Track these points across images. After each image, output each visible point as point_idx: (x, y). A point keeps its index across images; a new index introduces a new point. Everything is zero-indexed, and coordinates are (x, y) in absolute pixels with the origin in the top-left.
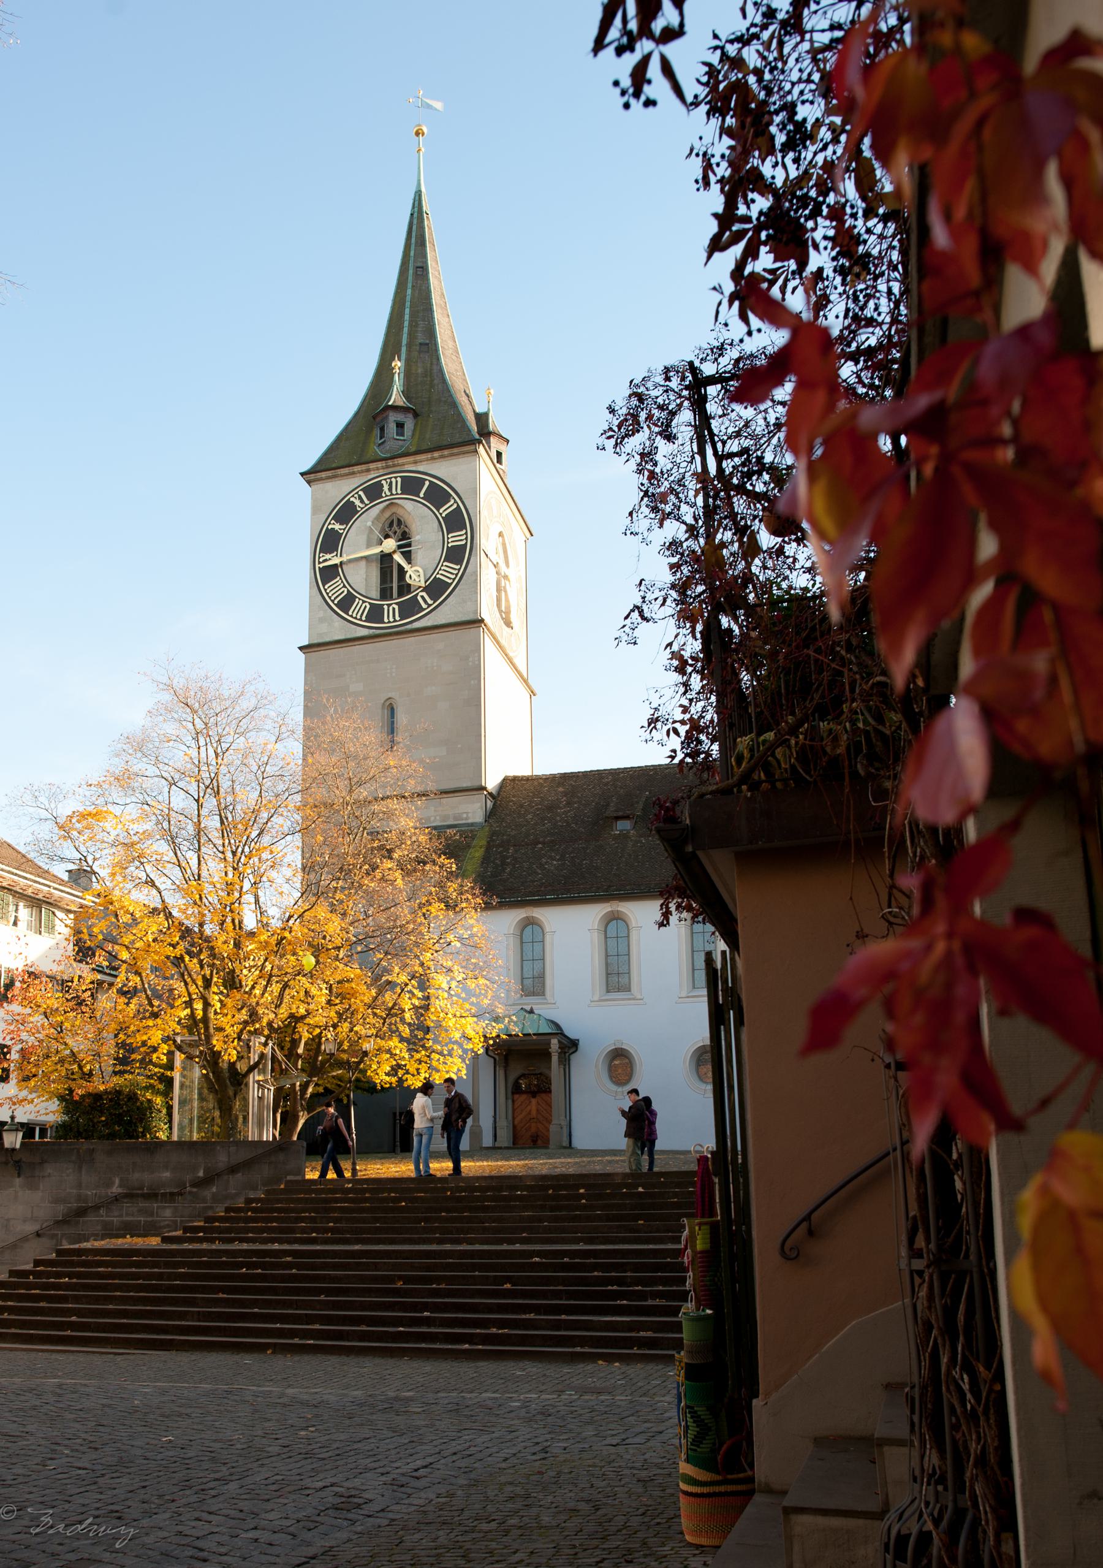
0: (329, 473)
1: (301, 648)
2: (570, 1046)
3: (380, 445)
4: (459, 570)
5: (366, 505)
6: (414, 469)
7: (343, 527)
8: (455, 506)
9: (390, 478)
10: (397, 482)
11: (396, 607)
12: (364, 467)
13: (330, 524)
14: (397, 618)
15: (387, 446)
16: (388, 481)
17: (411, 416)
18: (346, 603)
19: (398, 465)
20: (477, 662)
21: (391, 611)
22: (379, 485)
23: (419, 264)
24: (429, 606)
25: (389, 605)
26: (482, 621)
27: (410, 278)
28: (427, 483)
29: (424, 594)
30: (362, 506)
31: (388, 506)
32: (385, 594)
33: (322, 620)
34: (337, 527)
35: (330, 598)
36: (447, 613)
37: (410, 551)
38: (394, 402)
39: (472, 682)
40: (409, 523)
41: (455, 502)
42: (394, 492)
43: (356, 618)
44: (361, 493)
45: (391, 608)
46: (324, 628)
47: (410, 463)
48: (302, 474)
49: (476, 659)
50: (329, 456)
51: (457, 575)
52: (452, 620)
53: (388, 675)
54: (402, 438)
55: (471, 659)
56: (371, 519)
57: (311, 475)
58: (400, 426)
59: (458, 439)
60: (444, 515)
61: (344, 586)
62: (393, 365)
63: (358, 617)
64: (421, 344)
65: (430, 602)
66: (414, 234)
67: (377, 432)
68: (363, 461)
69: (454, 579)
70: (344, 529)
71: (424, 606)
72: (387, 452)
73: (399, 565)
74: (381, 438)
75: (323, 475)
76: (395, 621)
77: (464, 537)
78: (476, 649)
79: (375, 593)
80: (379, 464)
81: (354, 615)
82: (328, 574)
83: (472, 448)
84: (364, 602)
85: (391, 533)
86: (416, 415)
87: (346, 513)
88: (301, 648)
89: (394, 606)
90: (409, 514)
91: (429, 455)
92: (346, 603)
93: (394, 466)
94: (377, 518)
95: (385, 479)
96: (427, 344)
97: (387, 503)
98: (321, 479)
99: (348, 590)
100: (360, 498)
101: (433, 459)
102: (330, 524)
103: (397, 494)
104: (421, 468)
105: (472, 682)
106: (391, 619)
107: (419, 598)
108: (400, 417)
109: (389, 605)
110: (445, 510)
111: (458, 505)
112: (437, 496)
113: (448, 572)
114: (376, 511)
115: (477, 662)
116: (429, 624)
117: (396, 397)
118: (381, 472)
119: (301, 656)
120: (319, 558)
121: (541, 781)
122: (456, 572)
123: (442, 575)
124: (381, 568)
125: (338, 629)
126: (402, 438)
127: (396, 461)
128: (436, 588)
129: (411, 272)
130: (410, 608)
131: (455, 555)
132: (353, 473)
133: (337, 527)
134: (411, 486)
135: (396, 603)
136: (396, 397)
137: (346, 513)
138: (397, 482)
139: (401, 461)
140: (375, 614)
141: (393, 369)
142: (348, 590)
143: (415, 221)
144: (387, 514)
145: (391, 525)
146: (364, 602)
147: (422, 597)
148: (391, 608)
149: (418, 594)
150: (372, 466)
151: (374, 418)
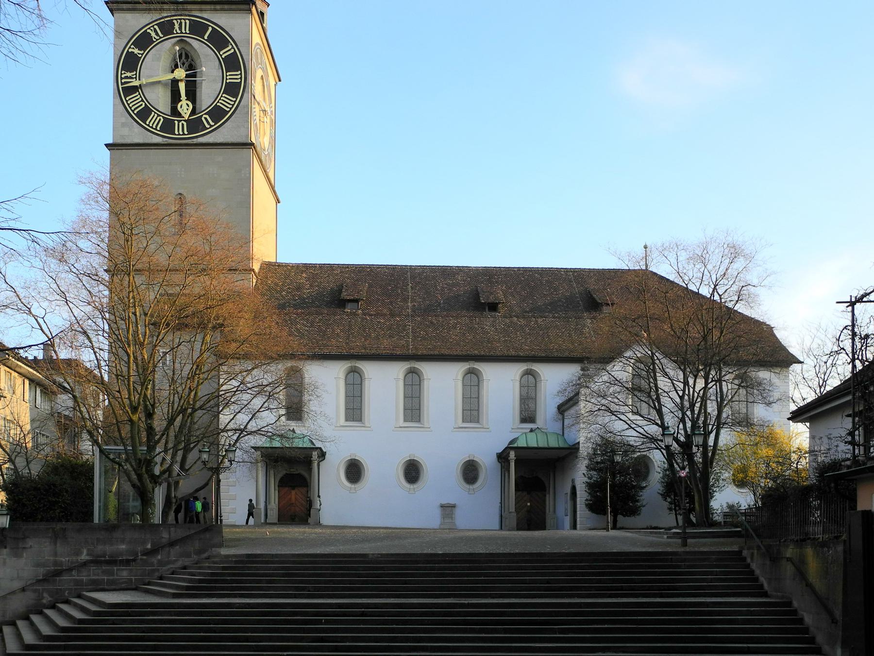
1: (107, 145)
4: (235, 102)
5: (161, 38)
8: (232, 51)
10: (186, 23)
12: (159, 6)
14: (186, 132)
16: (179, 21)
18: (144, 114)
20: (248, 175)
24: (211, 126)
25: (179, 121)
26: (252, 144)
28: (210, 29)
29: (207, 116)
30: (158, 38)
33: (124, 125)
34: (136, 51)
35: (130, 108)
36: (224, 134)
37: (196, 80)
39: (244, 190)
40: (195, 58)
41: (233, 48)
44: (156, 27)
45: (180, 124)
46: (125, 131)
49: (247, 172)
51: (233, 105)
53: (179, 176)
55: (243, 172)
61: (142, 100)
63: (154, 127)
65: (212, 124)
69: (231, 109)
70: (142, 54)
71: (208, 126)
76: (184, 134)
77: (239, 76)
78: (249, 166)
79: (168, 111)
87: (144, 41)
88: (107, 145)
97: (178, 39)
98: (123, 10)
100: (155, 30)
101: (216, 10)
102: (130, 48)
103: (186, 33)
104: (205, 15)
105: (244, 190)
106: (181, 133)
107: (203, 119)
109: (179, 121)
110: (225, 52)
112: (219, 40)
113: (226, 102)
114: (168, 44)
115: (248, 175)
118: (173, 13)
119: (107, 152)
120: (121, 74)
125: (137, 134)
127: (186, 6)
128: (217, 114)
131: (232, 89)
132: (150, 10)
133: (136, 51)
134: (198, 29)
137: (144, 41)
138: (186, 23)
139: (189, 7)
140: (168, 127)
146: (159, 115)
147: (206, 118)
149: (203, 115)
150: (165, 6)
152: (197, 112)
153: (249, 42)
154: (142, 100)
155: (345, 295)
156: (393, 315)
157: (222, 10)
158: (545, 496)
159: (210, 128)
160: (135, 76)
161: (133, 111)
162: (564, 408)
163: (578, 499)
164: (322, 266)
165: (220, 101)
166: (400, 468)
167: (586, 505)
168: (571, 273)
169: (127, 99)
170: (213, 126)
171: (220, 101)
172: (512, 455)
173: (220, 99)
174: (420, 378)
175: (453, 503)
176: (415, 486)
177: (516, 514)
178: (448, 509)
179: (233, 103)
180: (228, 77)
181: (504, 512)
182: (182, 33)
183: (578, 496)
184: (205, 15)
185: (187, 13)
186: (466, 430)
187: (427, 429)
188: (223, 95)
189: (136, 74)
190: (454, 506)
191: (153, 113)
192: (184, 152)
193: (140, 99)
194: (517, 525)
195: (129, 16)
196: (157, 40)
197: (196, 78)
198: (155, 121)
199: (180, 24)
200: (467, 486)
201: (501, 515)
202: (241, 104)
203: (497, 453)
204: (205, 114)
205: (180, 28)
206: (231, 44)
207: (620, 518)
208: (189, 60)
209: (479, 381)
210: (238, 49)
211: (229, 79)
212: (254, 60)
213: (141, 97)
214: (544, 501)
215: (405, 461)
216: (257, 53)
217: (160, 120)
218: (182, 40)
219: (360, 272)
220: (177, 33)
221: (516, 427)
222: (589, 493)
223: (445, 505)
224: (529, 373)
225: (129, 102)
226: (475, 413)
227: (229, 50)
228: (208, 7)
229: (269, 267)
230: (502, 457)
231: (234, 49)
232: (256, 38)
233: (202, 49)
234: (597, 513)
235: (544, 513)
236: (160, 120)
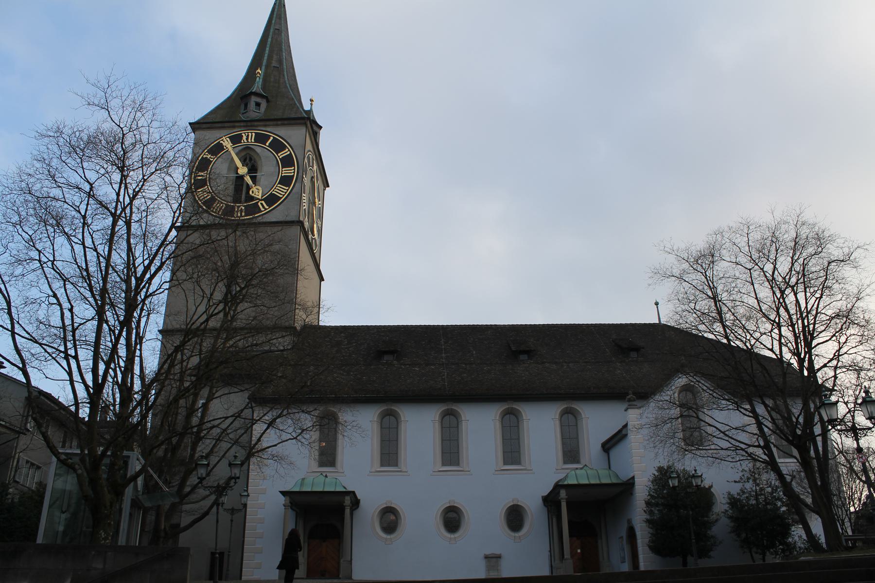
2: (356, 503)
3: (243, 114)
4: (288, 190)
6: (264, 129)
8: (289, 152)
10: (252, 135)
13: (205, 154)
15: (247, 115)
16: (247, 134)
17: (265, 100)
22: (240, 136)
23: (278, 28)
24: (266, 209)
26: (301, 224)
27: (271, 34)
28: (272, 138)
29: (263, 202)
31: (244, 148)
32: (237, 200)
34: (209, 156)
41: (289, 150)
50: (209, 116)
51: (286, 193)
57: (195, 126)
58: (258, 105)
59: (293, 116)
64: (274, 67)
66: (275, 13)
67: (243, 107)
68: (233, 119)
69: (284, 195)
71: (263, 209)
72: (248, 117)
73: (248, 184)
74: (245, 110)
75: (204, 126)
80: (242, 124)
83: (302, 121)
86: (268, 101)
90: (258, 154)
91: (275, 123)
92: (209, 203)
93: (251, 126)
95: (245, 133)
96: (278, 67)
97: (244, 146)
101: (277, 125)
102: (205, 154)
103: (251, 142)
104: (269, 129)
107: (259, 204)
108: (259, 100)
110: (282, 154)
111: (291, 152)
112: (277, 146)
113: (280, 191)
117: (257, 86)
121: (329, 329)
123: (276, 192)
128: (271, 199)
129: (272, 30)
133: (209, 156)
134: (261, 139)
136: (257, 86)
138: (252, 135)
139: (256, 124)
143: (277, 7)
147: (262, 204)
150: (237, 124)
151: (242, 98)
159: (265, 211)
162: (607, 446)
165: (275, 190)
171: (275, 190)
173: (275, 188)
175: (498, 552)
176: (457, 535)
178: (493, 559)
180: (283, 172)
182: (248, 142)
184: (269, 129)
185: (254, 128)
186: (508, 472)
187: (466, 473)
188: (278, 186)
190: (499, 557)
197: (256, 173)
199: (248, 136)
200: (513, 534)
201: (551, 565)
202: (293, 191)
203: (542, 497)
206: (288, 148)
208: (252, 162)
209: (518, 422)
211: (284, 173)
212: (306, 160)
215: (444, 508)
216: (308, 158)
220: (244, 142)
223: (490, 556)
227: (286, 152)
228: (271, 123)
230: (551, 501)
231: (290, 151)
233: (263, 152)
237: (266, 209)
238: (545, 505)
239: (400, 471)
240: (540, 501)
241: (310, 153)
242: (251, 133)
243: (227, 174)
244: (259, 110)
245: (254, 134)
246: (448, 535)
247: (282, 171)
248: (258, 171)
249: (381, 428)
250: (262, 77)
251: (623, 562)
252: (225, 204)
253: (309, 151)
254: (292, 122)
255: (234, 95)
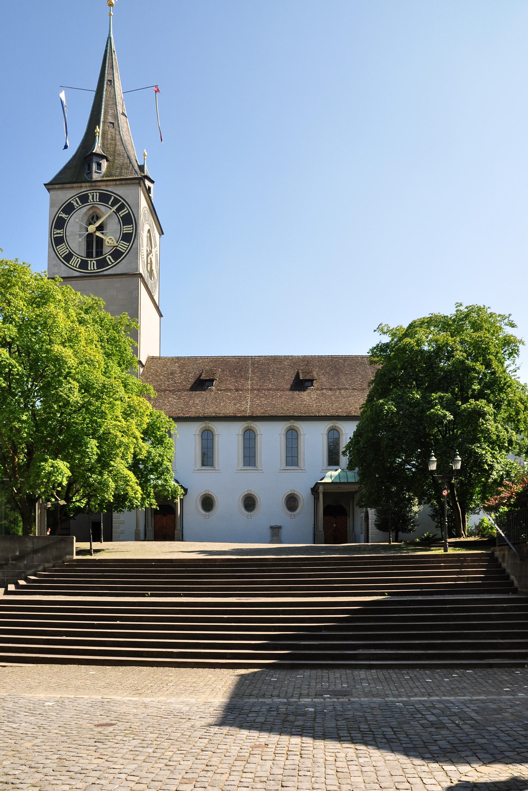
0: (60, 186)
3: (88, 174)
4: (129, 246)
7: (67, 216)
8: (127, 212)
9: (93, 193)
11: (95, 262)
12: (79, 185)
13: (60, 213)
16: (92, 194)
17: (105, 160)
18: (68, 257)
19: (97, 186)
21: (92, 264)
24: (113, 263)
25: (91, 261)
26: (141, 274)
28: (113, 198)
29: (110, 257)
30: (78, 206)
31: (91, 208)
32: (89, 254)
33: (55, 266)
34: (64, 216)
35: (59, 254)
38: (96, 151)
41: (128, 209)
42: (95, 200)
43: (73, 266)
44: (77, 199)
47: (103, 186)
48: (45, 185)
50: (60, 176)
51: (127, 248)
52: (124, 272)
54: (100, 171)
55: (134, 293)
56: (82, 214)
57: (50, 186)
60: (121, 216)
61: (67, 248)
62: (95, 131)
63: (75, 266)
65: (113, 261)
69: (126, 251)
70: (68, 218)
71: (110, 263)
74: (88, 170)
75: (57, 186)
76: (94, 270)
77: (132, 229)
78: (137, 288)
79: (84, 254)
80: (87, 184)
81: (72, 265)
82: (58, 241)
83: (137, 181)
84: (78, 258)
85: (92, 222)
87: (69, 209)
89: (94, 261)
90: (103, 213)
91: (114, 183)
92: (68, 257)
93: (95, 186)
94: (86, 213)
95: (90, 193)
97: (91, 206)
98: (55, 189)
99: (69, 251)
100: (76, 201)
101: (116, 185)
102: (60, 213)
103: (97, 201)
105: (134, 306)
106: (92, 269)
107: (107, 259)
109: (91, 261)
111: (129, 211)
113: (123, 246)
114: (85, 210)
116: (112, 273)
117: (97, 149)
120: (54, 231)
122: (127, 247)
124: (87, 241)
126: (100, 171)
128: (117, 254)
130: (102, 264)
131: (127, 238)
132: (73, 188)
133: (64, 216)
134: (104, 198)
135: (95, 260)
137: (69, 209)
139: (99, 184)
140: (84, 265)
141: (96, 133)
142: (69, 251)
144: (91, 212)
145: (93, 218)
146: (78, 258)
147: (109, 258)
148: (92, 262)
149: (106, 256)
150: (83, 185)
151: (85, 158)
152: (103, 254)
153: (138, 205)
154: (67, 248)
155: (203, 377)
156: (237, 390)
157: (121, 184)
158: (347, 519)
159: (112, 264)
160: (62, 232)
161: (61, 256)
163: (370, 521)
164: (189, 358)
166: (241, 499)
167: (375, 524)
168: (365, 359)
169: (57, 248)
170: (113, 263)
172: (321, 488)
174: (255, 433)
177: (323, 533)
179: (127, 247)
180: (124, 230)
181: (317, 531)
182: (94, 201)
183: (370, 518)
186: (289, 471)
189: (63, 231)
190: (280, 528)
191: (74, 256)
192: (94, 281)
193: (66, 248)
194: (325, 541)
195: (59, 193)
196: (77, 207)
197: (103, 230)
198: (75, 261)
200: (290, 513)
202: (133, 247)
203: (311, 488)
204: (109, 255)
205: (93, 199)
207: (400, 533)
209: (298, 435)
210: (131, 210)
211: (125, 230)
213: (66, 246)
214: (346, 523)
217: (78, 261)
218: (94, 206)
219: (215, 361)
221: (324, 469)
222: (378, 516)
224: (333, 430)
225: (58, 250)
226: (295, 459)
229: (151, 359)
232: (143, 203)
234: (383, 531)
235: (346, 532)
236: (78, 261)
237: (113, 263)
238: (312, 494)
239: (215, 470)
240: (310, 491)
241: (146, 209)
242: (96, 192)
243: (79, 232)
244: (101, 170)
245: (98, 194)
246: (246, 513)
247: (123, 228)
248: (104, 229)
249: (202, 439)
250: (100, 134)
251: (362, 533)
252: (81, 259)
253: (145, 207)
254: (128, 182)
255: (79, 153)
